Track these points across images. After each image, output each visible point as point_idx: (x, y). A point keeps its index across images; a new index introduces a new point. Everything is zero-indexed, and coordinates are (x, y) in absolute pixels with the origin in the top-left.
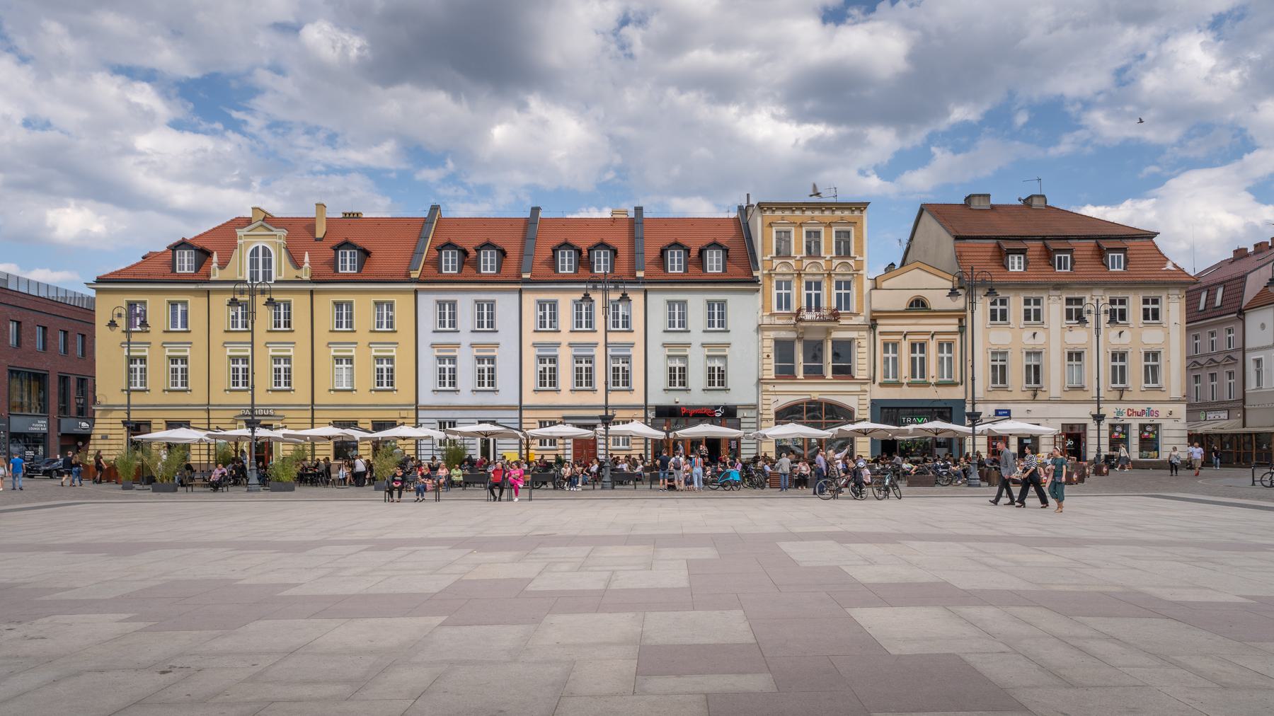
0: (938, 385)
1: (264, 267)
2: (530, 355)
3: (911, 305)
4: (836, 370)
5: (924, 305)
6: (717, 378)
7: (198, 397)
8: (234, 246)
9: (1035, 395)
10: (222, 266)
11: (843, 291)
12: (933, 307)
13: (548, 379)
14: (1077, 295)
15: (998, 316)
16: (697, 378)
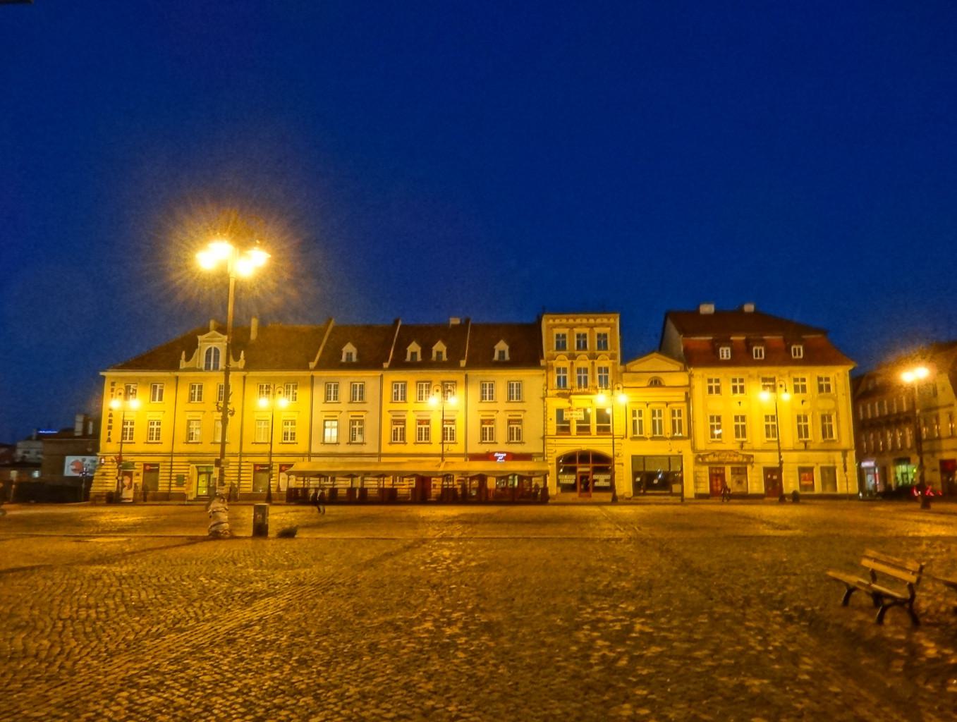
0: (673, 438)
1: (214, 361)
2: (387, 418)
3: (652, 382)
4: (599, 429)
5: (660, 383)
6: (515, 434)
7: (165, 447)
8: (197, 347)
9: (742, 446)
10: (188, 359)
11: (603, 374)
12: (667, 384)
13: (398, 436)
14: (768, 376)
15: (714, 390)
16: (501, 432)
